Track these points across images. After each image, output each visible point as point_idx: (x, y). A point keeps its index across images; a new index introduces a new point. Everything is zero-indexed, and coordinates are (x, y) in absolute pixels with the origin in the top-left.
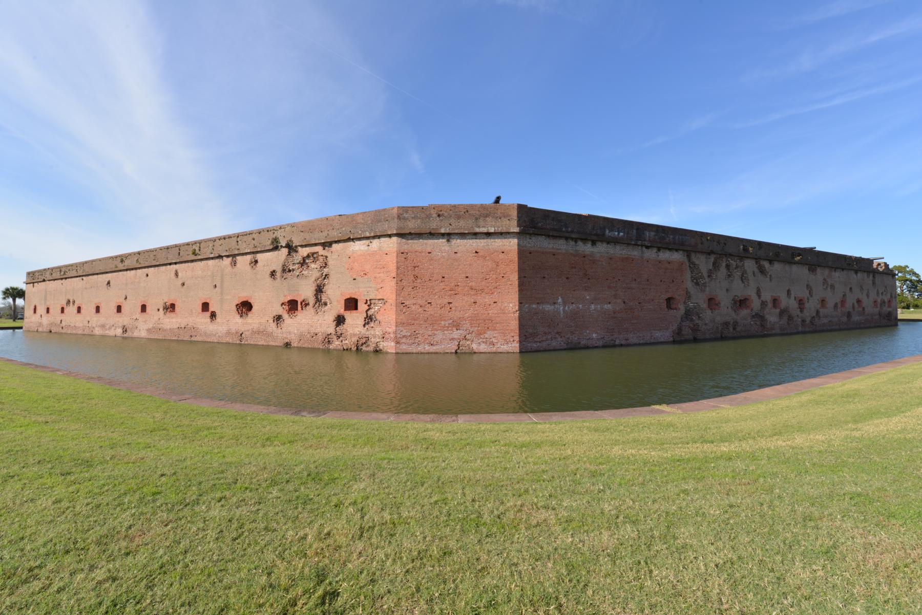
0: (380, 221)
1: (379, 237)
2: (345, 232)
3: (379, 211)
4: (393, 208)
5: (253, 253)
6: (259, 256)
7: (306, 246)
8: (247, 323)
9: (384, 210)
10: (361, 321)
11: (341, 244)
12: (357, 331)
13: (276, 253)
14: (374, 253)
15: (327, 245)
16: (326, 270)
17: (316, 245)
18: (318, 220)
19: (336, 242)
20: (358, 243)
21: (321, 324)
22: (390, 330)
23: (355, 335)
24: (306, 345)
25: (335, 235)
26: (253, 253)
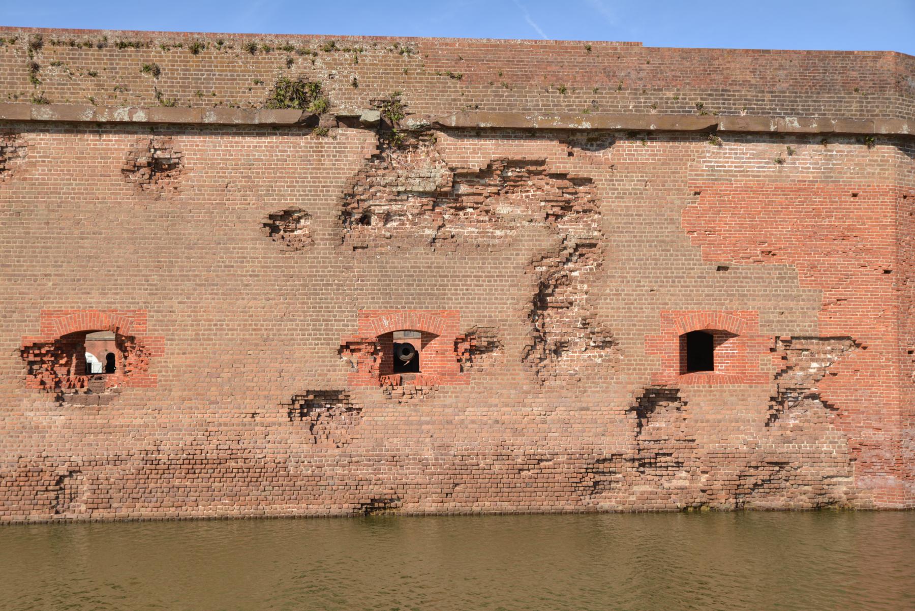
0: (825, 87)
1: (826, 138)
2: (683, 99)
3: (823, 56)
4: (878, 56)
5: (151, 127)
6: (187, 147)
7: (478, 132)
8: (107, 430)
9: (845, 55)
10: (757, 405)
11: (657, 147)
12: (738, 442)
13: (303, 142)
14: (802, 189)
15: (599, 138)
16: (573, 230)
17: (532, 133)
18: (537, 45)
19: (632, 134)
20: (731, 147)
21: (567, 423)
22: (880, 436)
23: (729, 457)
24: (486, 505)
25: (625, 108)
26: (151, 127)
